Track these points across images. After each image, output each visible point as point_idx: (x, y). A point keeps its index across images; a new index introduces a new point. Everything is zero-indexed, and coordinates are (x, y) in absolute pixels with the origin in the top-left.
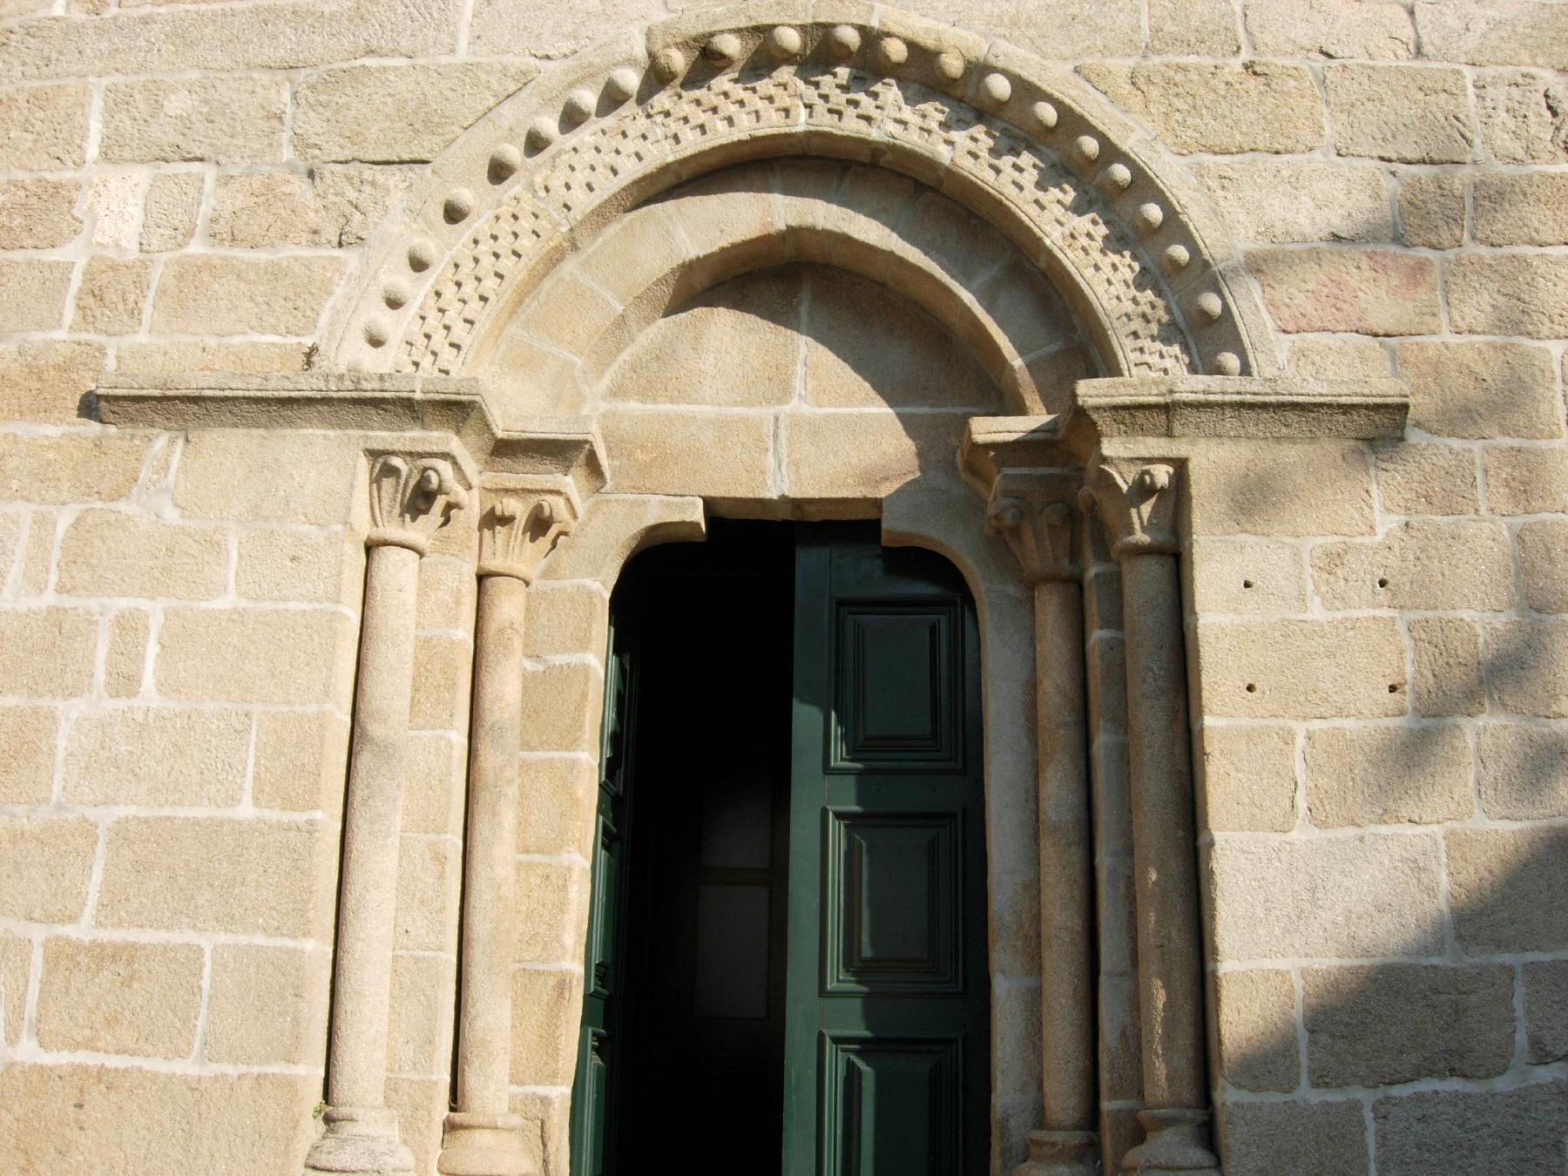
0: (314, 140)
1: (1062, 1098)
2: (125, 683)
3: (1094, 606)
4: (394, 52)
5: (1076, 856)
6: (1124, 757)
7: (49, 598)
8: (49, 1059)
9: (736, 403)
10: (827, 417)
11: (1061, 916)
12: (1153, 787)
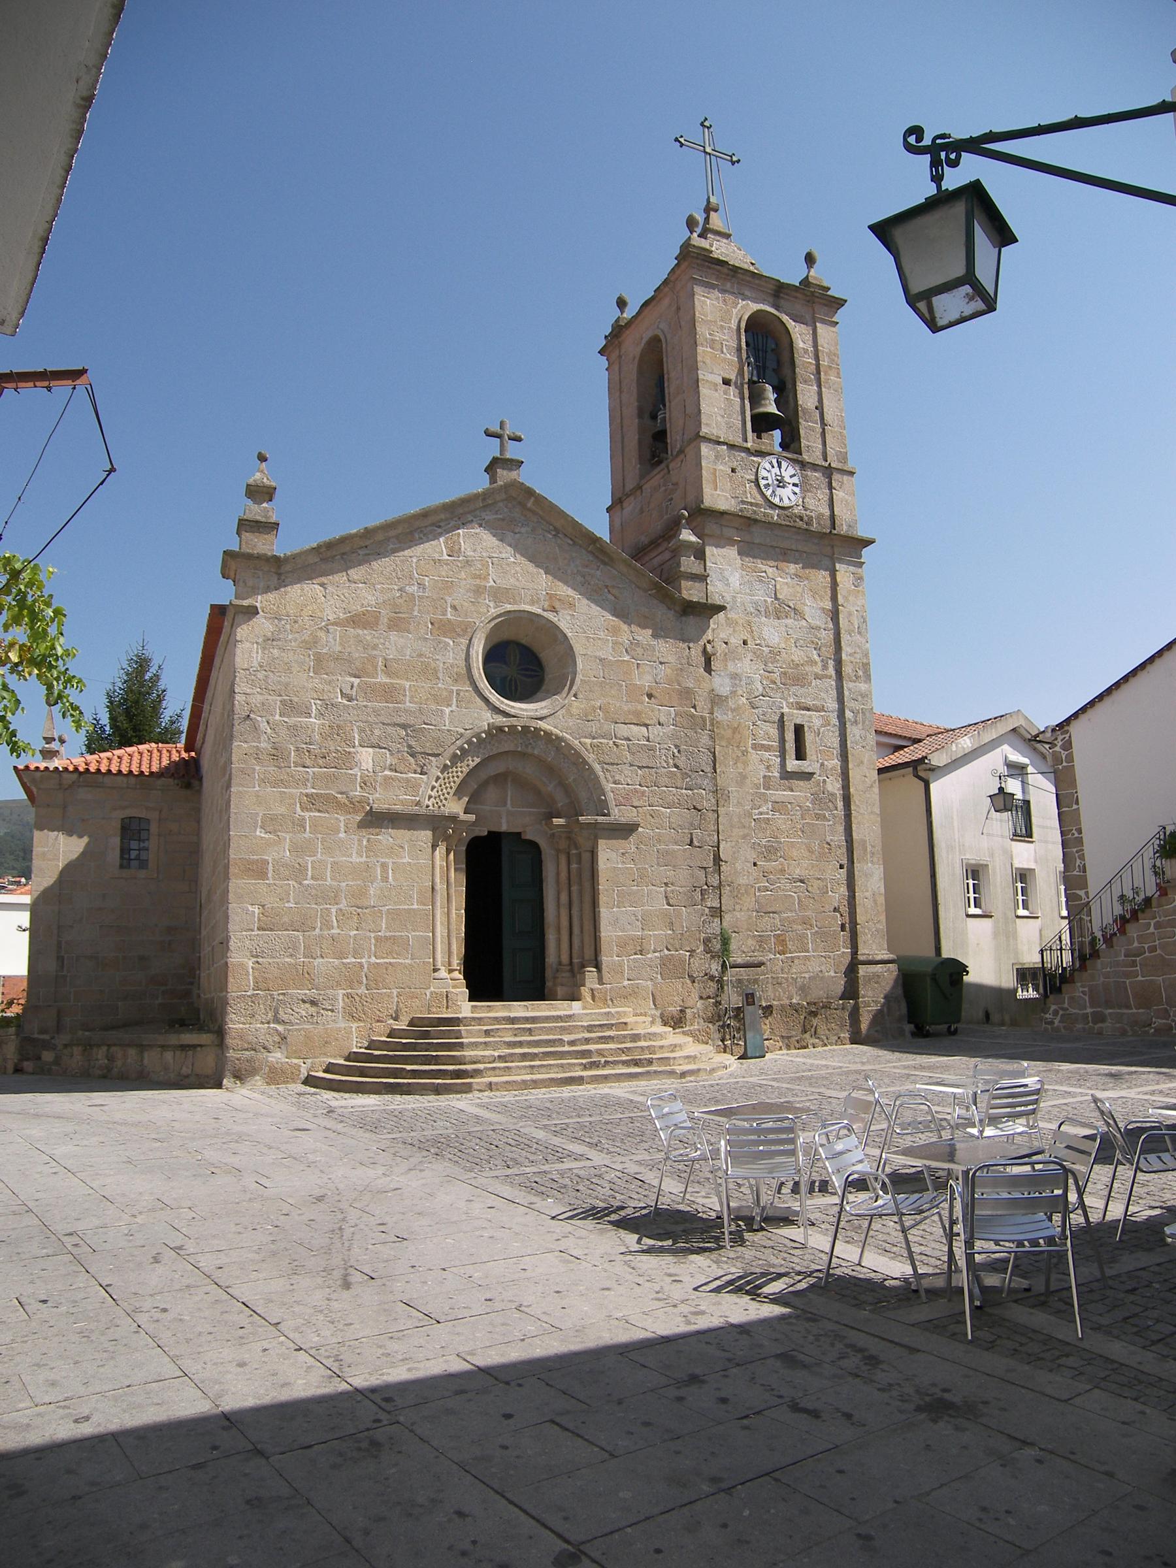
1: (565, 958)
2: (385, 879)
3: (574, 859)
4: (431, 725)
5: (568, 911)
6: (581, 892)
7: (364, 859)
8: (378, 961)
11: (565, 922)
12: (587, 898)
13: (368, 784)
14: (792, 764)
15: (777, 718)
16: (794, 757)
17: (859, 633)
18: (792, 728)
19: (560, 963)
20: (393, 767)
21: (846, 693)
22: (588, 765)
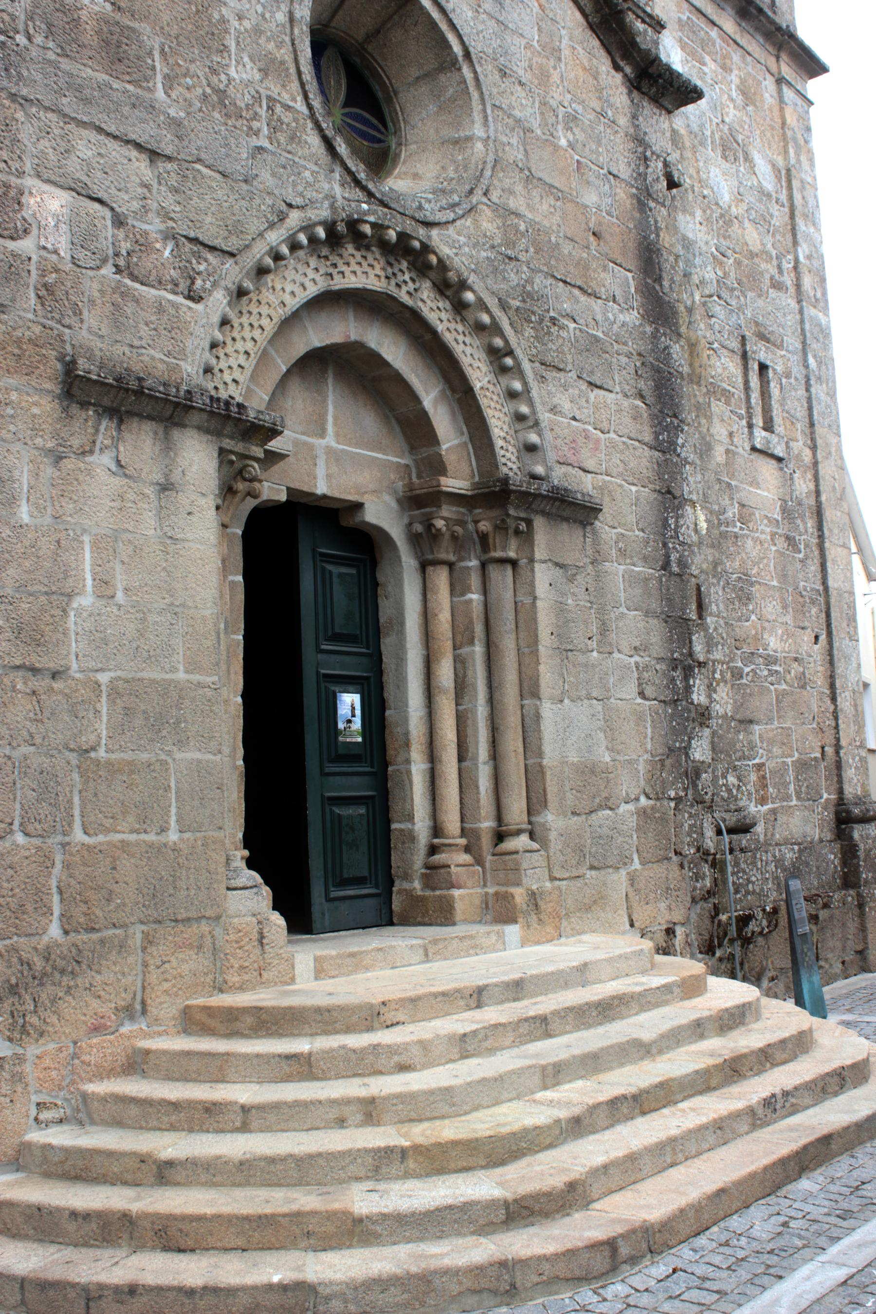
0: (172, 215)
1: (452, 822)
9: (303, 434)
10: (342, 451)
13: (60, 294)
14: (760, 435)
15: (735, 344)
16: (761, 424)
17: (814, 225)
18: (756, 367)
19: (437, 830)
20: (121, 262)
21: (807, 326)
22: (515, 358)
